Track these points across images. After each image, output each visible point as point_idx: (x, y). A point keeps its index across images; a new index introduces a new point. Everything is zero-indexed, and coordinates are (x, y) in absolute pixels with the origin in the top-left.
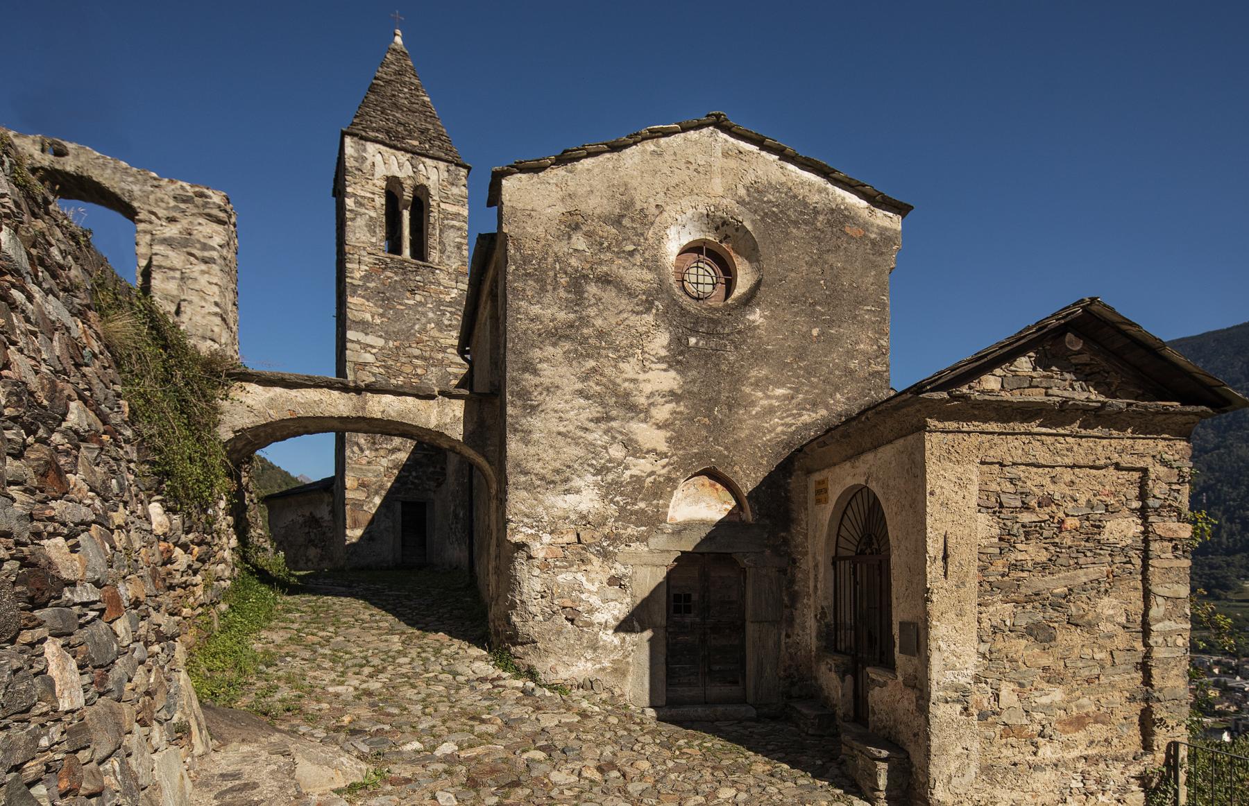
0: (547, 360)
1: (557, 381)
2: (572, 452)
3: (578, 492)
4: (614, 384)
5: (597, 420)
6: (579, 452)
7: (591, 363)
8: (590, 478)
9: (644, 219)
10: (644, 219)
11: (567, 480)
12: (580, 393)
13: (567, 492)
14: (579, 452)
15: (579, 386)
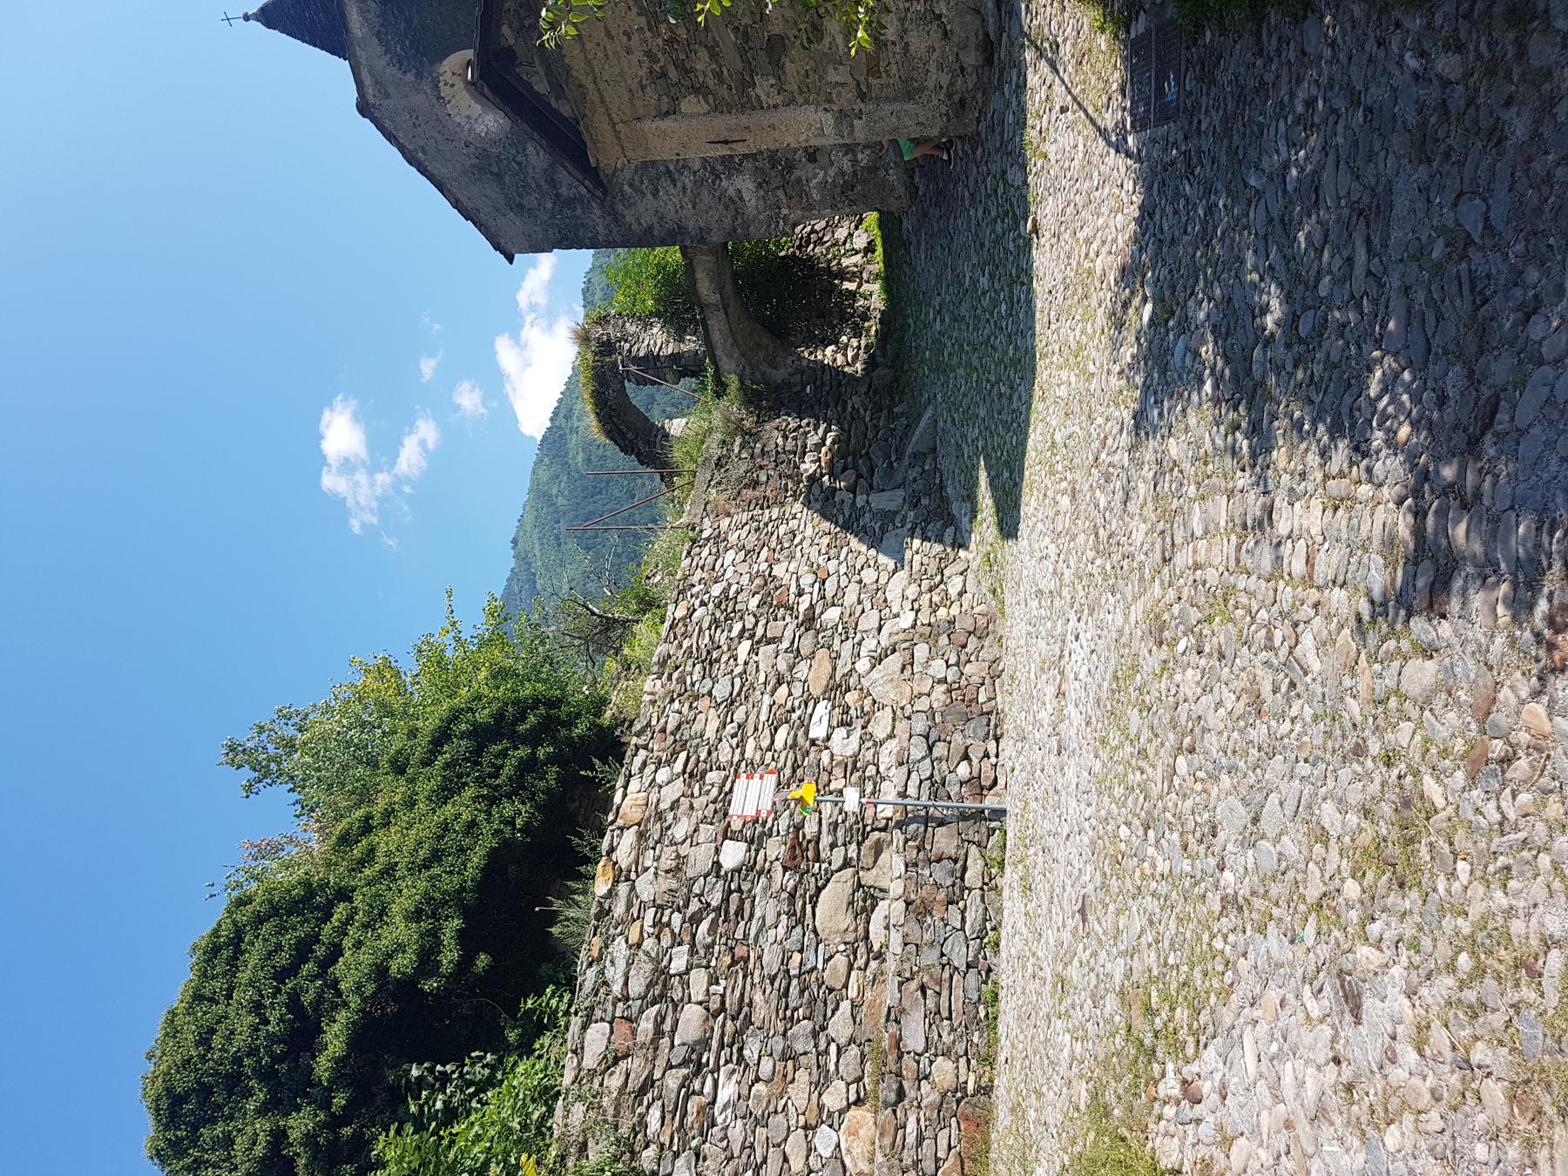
0: (637, 219)
1: (652, 212)
2: (705, 196)
3: (739, 191)
4: (636, 172)
5: (674, 182)
6: (705, 192)
7: (626, 187)
8: (725, 183)
9: (483, 155)
10: (483, 155)
11: (731, 199)
12: (655, 193)
13: (741, 198)
14: (705, 192)
15: (650, 196)
